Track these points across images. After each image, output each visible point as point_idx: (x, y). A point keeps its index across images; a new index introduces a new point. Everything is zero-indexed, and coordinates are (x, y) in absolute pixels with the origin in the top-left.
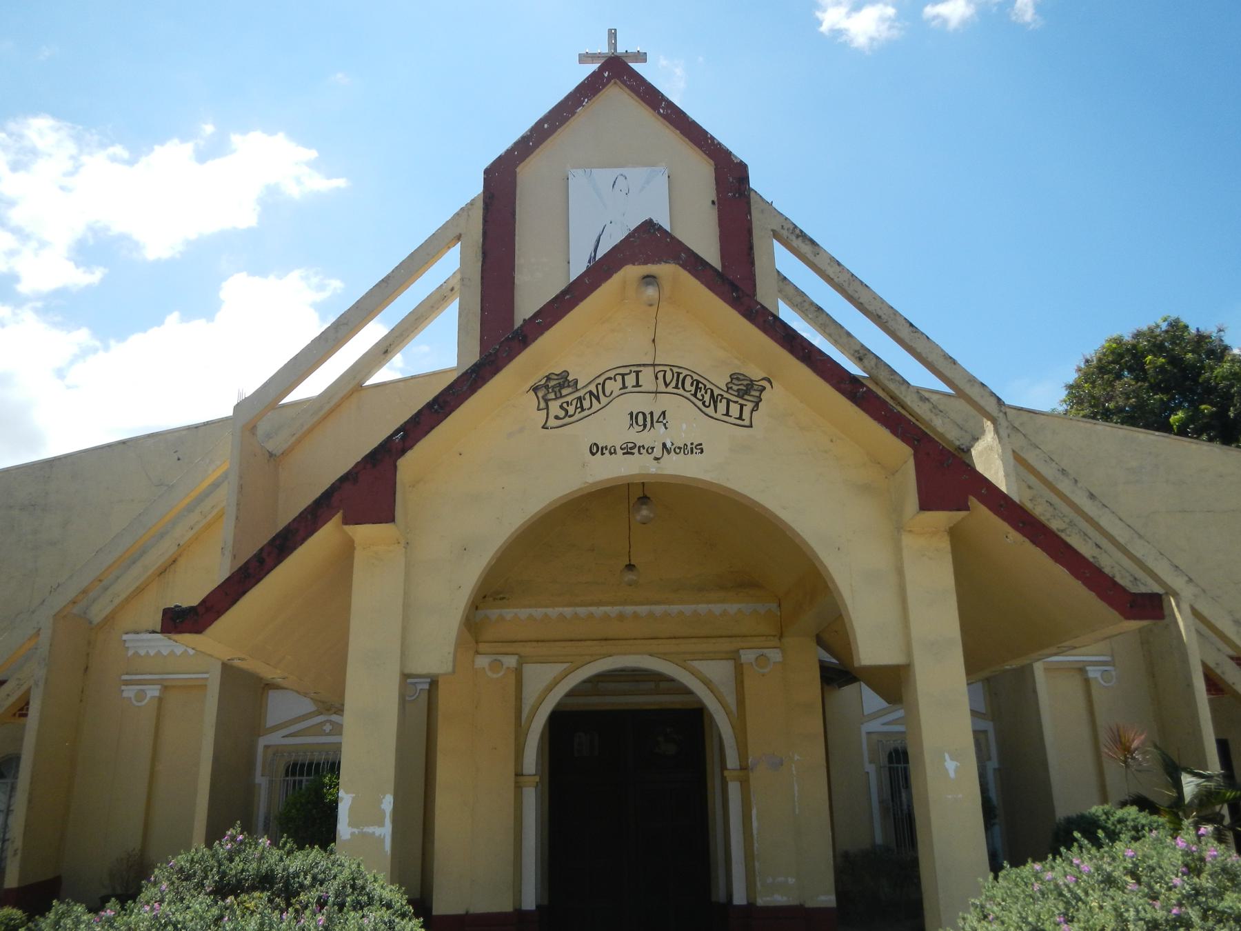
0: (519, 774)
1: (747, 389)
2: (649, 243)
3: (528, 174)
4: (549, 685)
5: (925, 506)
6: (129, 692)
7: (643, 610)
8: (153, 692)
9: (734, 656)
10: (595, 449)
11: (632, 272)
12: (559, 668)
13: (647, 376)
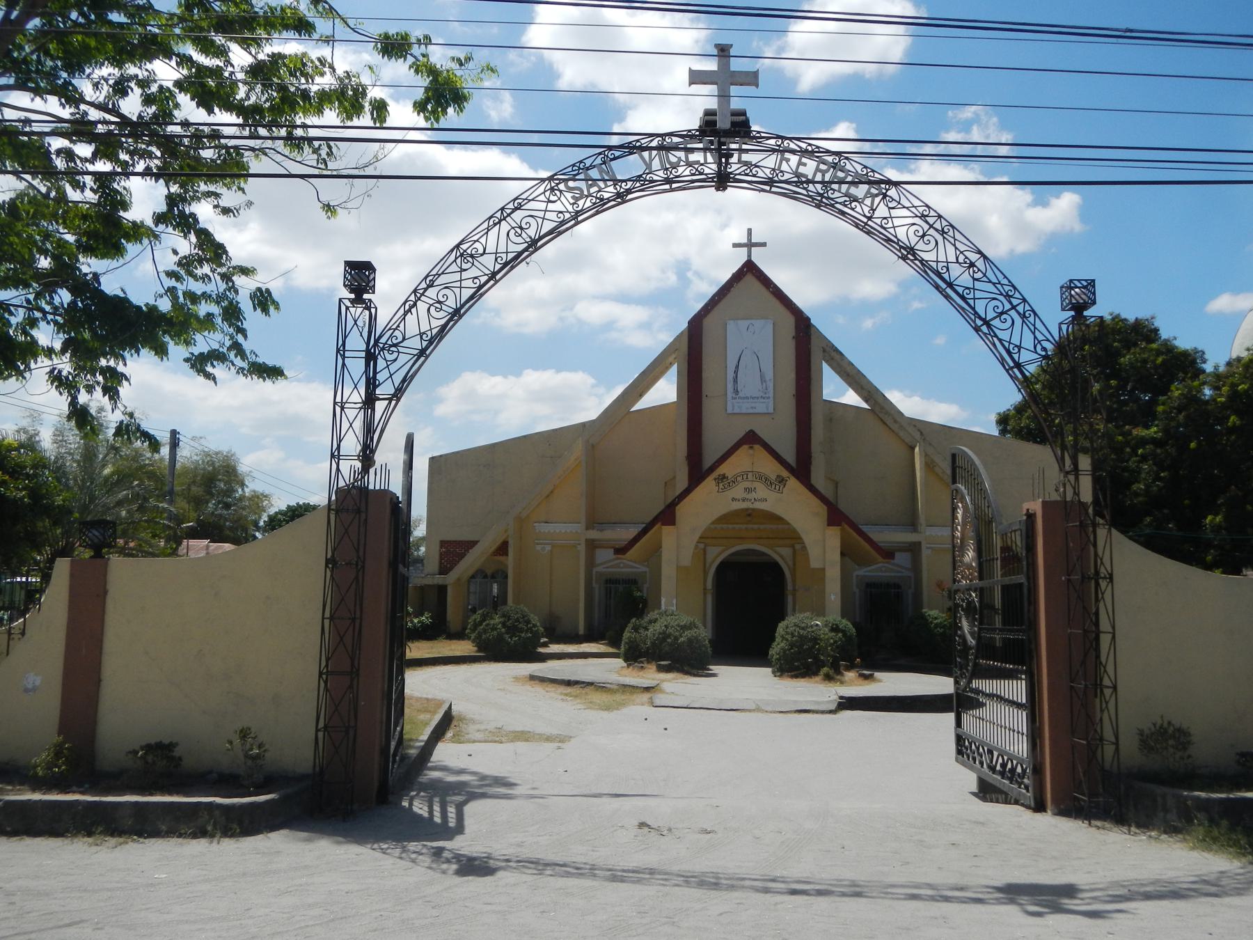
0: (705, 589)
1: (782, 480)
2: (751, 439)
3: (708, 322)
4: (717, 555)
5: (829, 525)
6: (539, 548)
7: (756, 526)
8: (548, 548)
9: (793, 546)
10: (733, 499)
11: (746, 447)
12: (721, 548)
13: (750, 475)
